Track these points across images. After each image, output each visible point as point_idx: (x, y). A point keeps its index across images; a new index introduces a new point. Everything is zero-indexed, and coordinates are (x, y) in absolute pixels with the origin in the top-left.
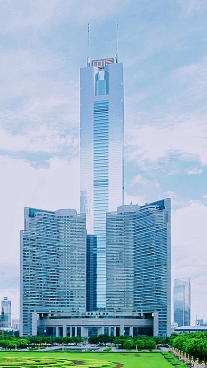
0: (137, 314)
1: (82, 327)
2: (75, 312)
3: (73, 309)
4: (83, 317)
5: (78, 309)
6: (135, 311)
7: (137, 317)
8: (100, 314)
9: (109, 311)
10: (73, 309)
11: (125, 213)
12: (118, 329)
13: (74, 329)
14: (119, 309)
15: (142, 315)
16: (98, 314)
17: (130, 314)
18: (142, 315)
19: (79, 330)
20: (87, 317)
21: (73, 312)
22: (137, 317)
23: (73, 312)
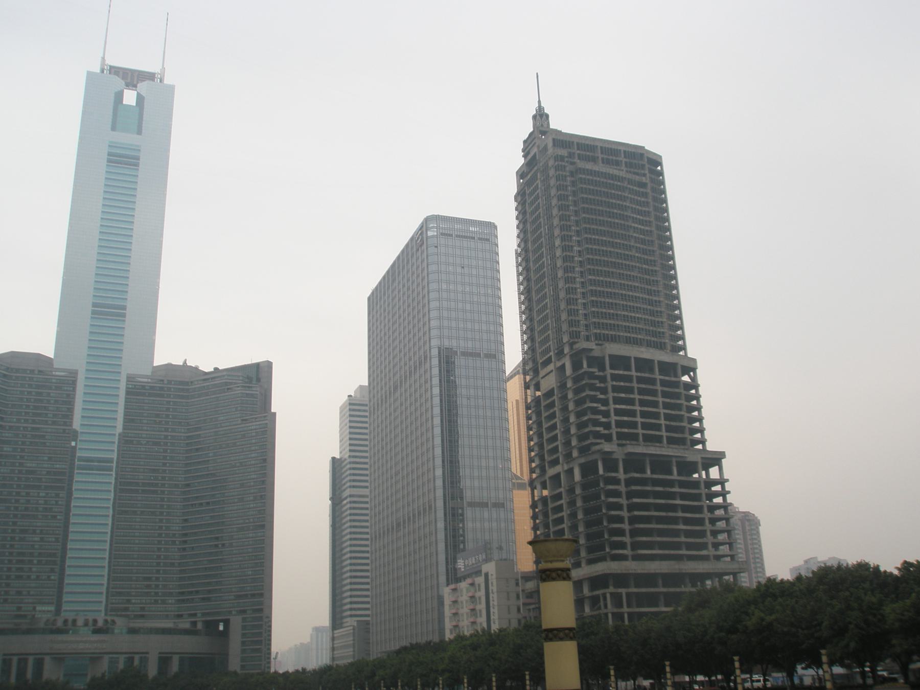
0: (185, 625)
1: (47, 659)
2: (25, 616)
3: (19, 609)
4: (44, 631)
5: (34, 608)
6: (180, 616)
7: (186, 632)
8: (95, 621)
9: (117, 616)
10: (19, 609)
11: (170, 382)
12: (144, 661)
13: (23, 662)
14: (143, 609)
15: (200, 626)
16: (91, 622)
17: (168, 624)
18: (200, 626)
19: (39, 664)
20: (59, 631)
21: (17, 616)
22: (186, 632)
23: (17, 616)
